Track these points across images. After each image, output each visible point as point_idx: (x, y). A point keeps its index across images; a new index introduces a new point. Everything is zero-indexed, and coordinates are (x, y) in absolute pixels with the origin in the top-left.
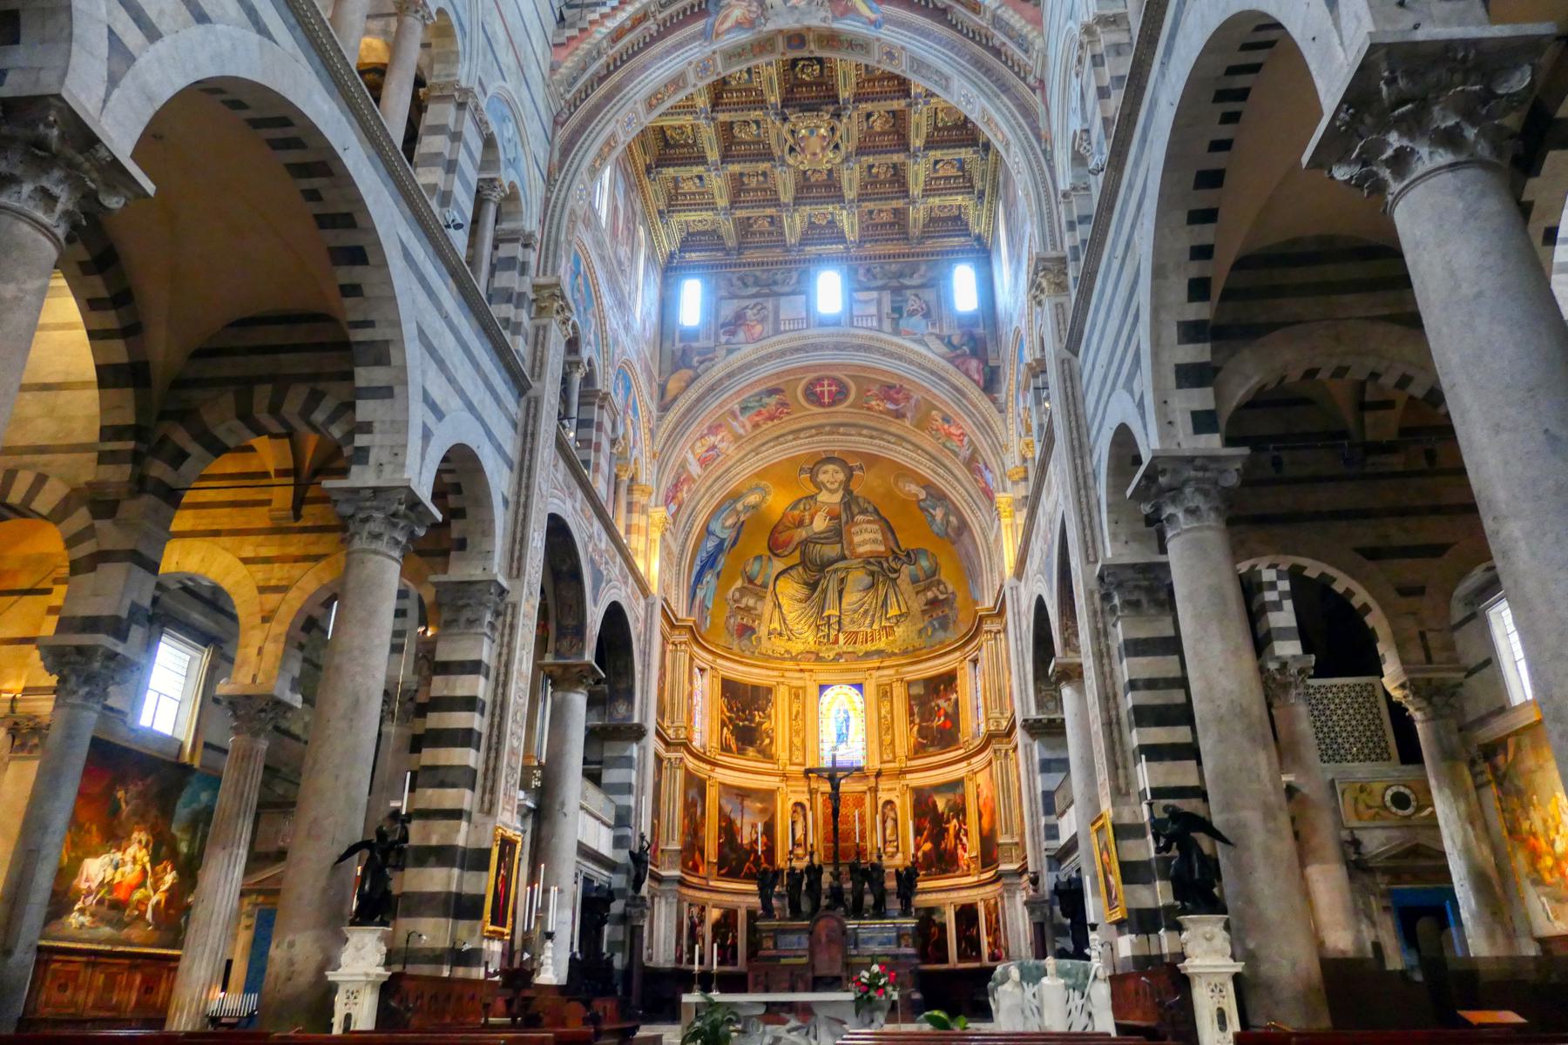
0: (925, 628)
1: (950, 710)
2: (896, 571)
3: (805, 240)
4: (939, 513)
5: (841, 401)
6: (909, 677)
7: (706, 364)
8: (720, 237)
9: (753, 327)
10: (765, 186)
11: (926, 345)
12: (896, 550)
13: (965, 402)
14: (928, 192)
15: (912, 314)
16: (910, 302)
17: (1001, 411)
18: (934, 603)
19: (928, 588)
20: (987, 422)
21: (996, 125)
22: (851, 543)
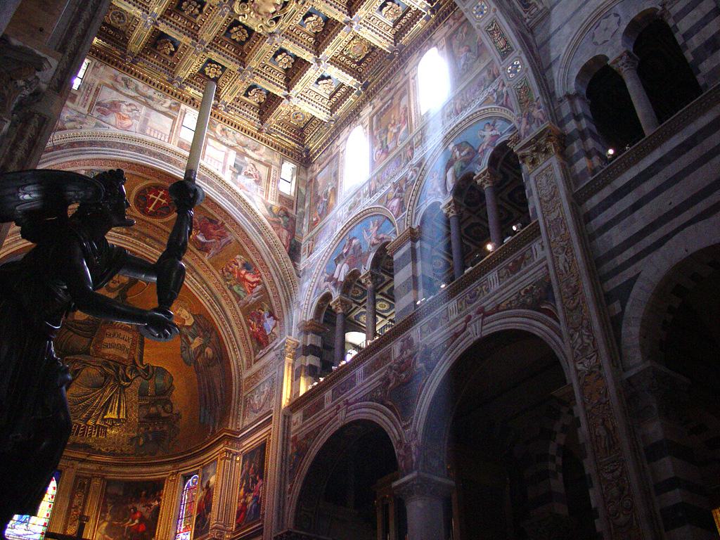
0: (138, 437)
1: (147, 515)
2: (128, 380)
3: (188, 82)
4: (196, 343)
5: (162, 216)
6: (111, 476)
7: (75, 123)
8: (126, 41)
9: (124, 119)
10: (193, 19)
11: (254, 202)
12: (137, 361)
13: (272, 256)
14: (301, 97)
15: (249, 175)
16: (248, 168)
17: (299, 276)
18: (156, 417)
19: (153, 405)
20: (287, 281)
21: (502, 35)
22: (101, 341)
